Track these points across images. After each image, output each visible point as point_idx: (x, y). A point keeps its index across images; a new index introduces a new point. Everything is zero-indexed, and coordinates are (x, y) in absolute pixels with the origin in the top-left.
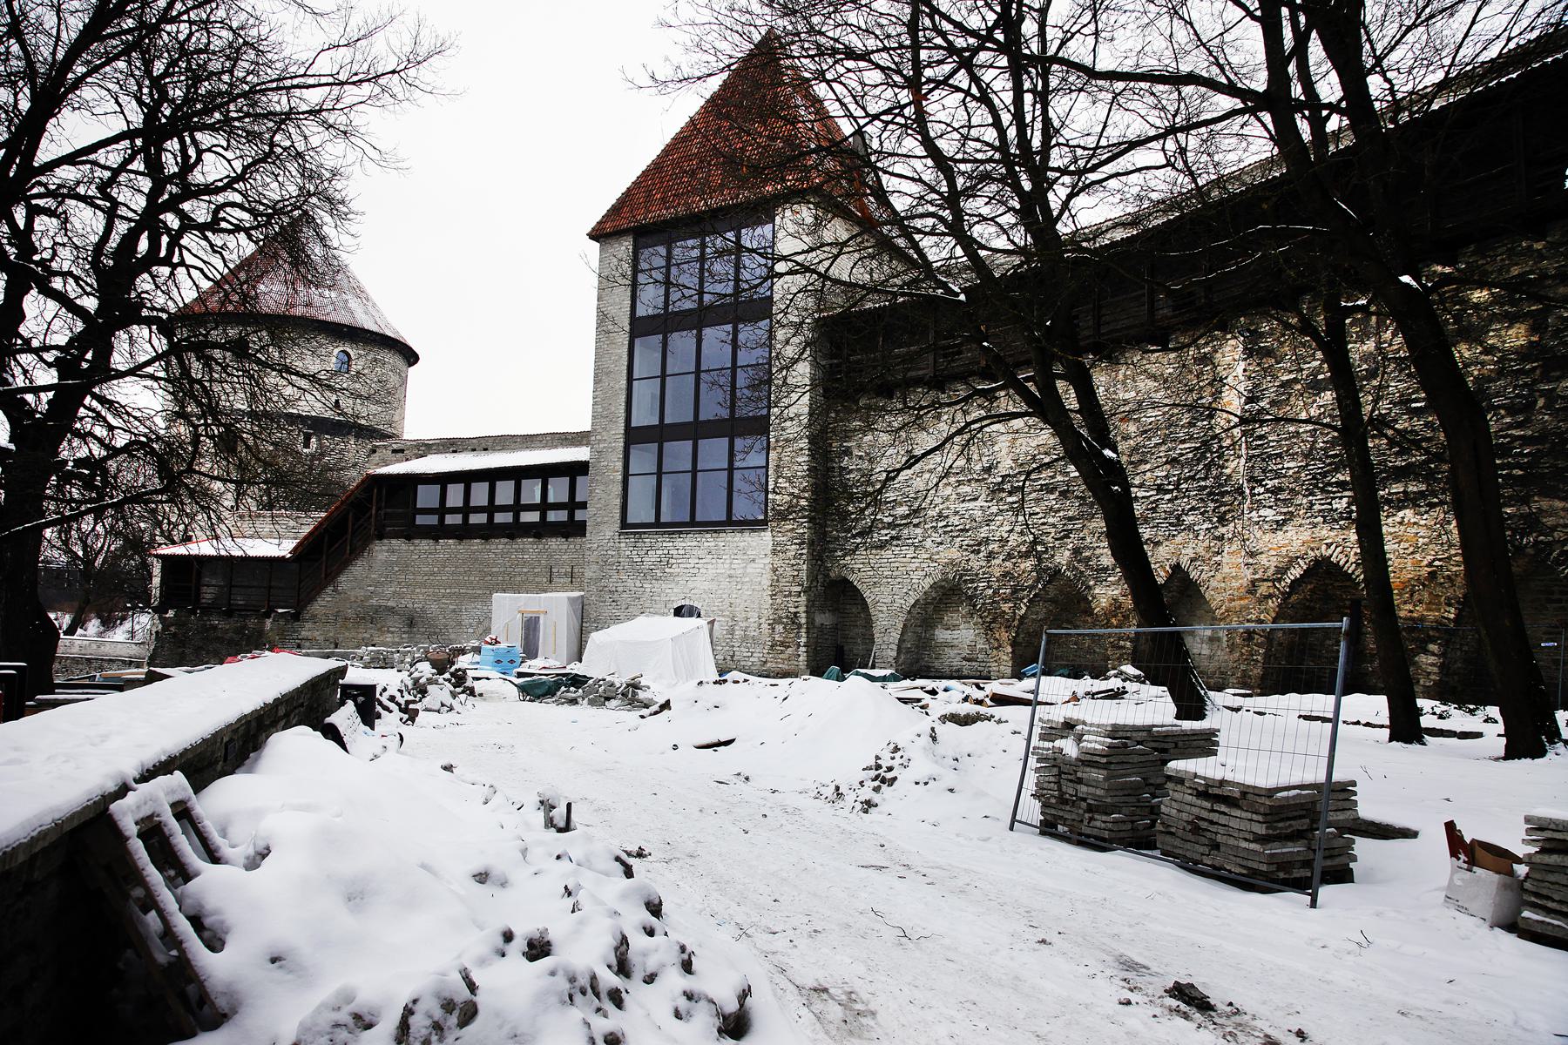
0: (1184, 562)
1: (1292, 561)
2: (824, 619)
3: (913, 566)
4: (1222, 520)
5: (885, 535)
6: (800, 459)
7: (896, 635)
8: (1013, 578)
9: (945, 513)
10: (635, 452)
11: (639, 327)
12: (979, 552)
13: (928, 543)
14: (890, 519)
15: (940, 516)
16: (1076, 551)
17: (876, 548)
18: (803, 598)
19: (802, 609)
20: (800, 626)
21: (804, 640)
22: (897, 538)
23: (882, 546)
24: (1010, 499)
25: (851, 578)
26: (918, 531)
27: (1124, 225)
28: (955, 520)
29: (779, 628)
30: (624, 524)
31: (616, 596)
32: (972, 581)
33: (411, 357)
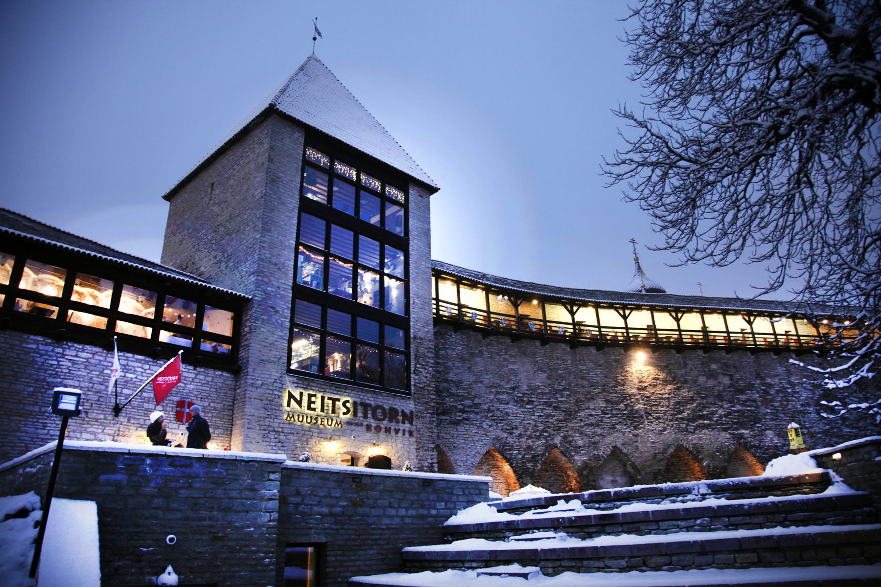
0: (619, 445)
1: (669, 446)
4: (636, 428)
5: (459, 416)
6: (430, 355)
8: (533, 450)
9: (492, 408)
12: (512, 433)
15: (489, 411)
16: (565, 437)
19: (435, 461)
22: (467, 419)
23: (457, 423)
24: (528, 406)
27: (492, 286)
31: (282, 437)
32: (510, 450)
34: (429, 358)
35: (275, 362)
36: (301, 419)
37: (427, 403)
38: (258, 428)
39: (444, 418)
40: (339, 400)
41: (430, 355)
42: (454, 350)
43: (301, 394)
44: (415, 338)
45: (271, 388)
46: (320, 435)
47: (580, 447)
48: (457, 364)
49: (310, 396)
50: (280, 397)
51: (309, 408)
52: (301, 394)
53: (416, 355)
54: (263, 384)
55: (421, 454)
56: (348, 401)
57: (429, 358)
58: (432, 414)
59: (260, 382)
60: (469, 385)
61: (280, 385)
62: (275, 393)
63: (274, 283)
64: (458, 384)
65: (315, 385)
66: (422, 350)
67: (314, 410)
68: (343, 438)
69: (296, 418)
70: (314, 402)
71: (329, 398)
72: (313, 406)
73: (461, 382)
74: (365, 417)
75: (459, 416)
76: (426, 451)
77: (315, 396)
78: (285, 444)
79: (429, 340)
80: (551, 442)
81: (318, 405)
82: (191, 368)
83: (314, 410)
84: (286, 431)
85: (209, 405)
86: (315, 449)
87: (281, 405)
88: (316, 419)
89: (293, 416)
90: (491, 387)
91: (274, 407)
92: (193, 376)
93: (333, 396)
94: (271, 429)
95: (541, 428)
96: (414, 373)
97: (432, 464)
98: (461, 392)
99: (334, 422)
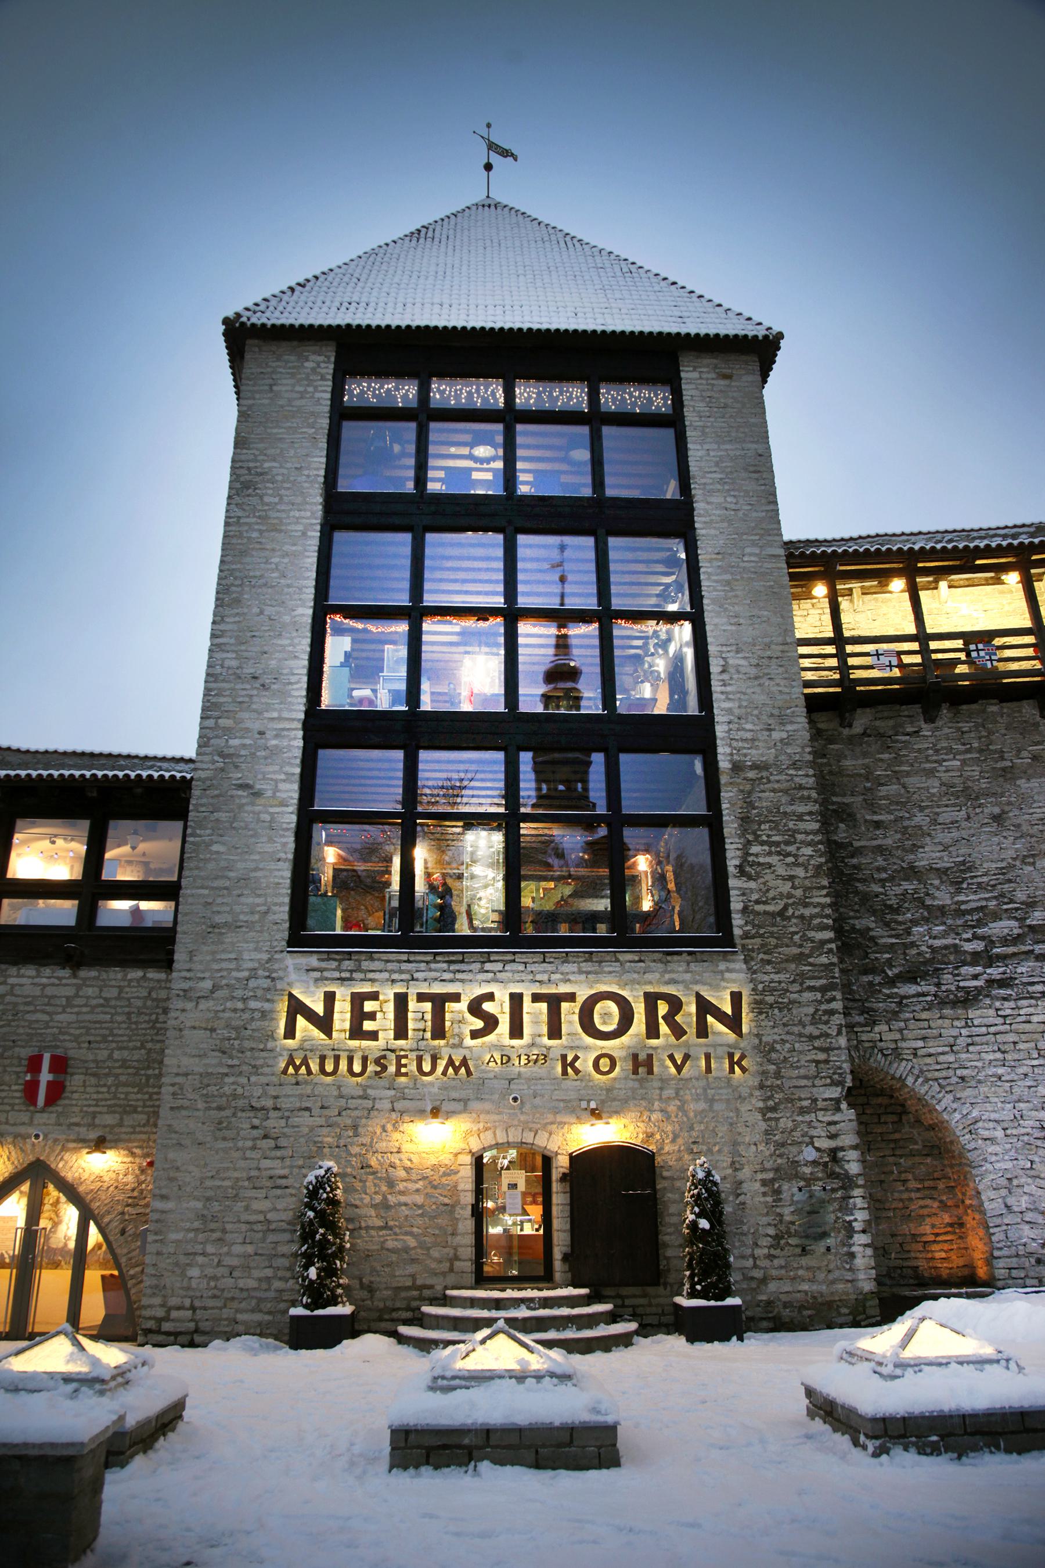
5: (972, 978)
6: (801, 809)
14: (978, 946)
17: (955, 1004)
18: (848, 1114)
19: (849, 1139)
20: (847, 1182)
21: (860, 1217)
22: (1004, 983)
23: (968, 999)
29: (790, 1190)
31: (274, 1123)
34: (800, 818)
35: (250, 925)
36: (329, 1068)
37: (800, 958)
38: (201, 1105)
39: (912, 989)
40: (456, 998)
41: (801, 809)
42: (931, 773)
43: (330, 999)
44: (737, 768)
45: (239, 993)
46: (398, 1105)
49: (358, 1000)
50: (266, 1015)
51: (356, 1032)
52: (330, 999)
53: (745, 820)
54: (215, 988)
55: (785, 1123)
56: (490, 997)
57: (800, 818)
58: (823, 989)
59: (208, 984)
60: (1002, 871)
61: (266, 983)
62: (253, 1004)
63: (248, 724)
64: (957, 876)
65: (377, 965)
66: (765, 799)
67: (373, 1035)
68: (474, 1105)
69: (314, 1067)
70: (372, 1016)
71: (421, 998)
72: (368, 1026)
73: (966, 867)
75: (972, 978)
76: (803, 1111)
77: (374, 996)
78: (282, 1142)
79: (794, 765)
81: (384, 1022)
82: (66, 973)
83: (373, 1035)
84: (285, 1104)
85: (110, 1057)
86: (382, 1146)
87: (272, 1036)
88: (377, 1062)
89: (305, 1062)
91: (247, 1044)
92: (70, 992)
93: (438, 989)
94: (241, 1103)
96: (742, 872)
97: (833, 1152)
98: (972, 899)
99: (441, 1065)
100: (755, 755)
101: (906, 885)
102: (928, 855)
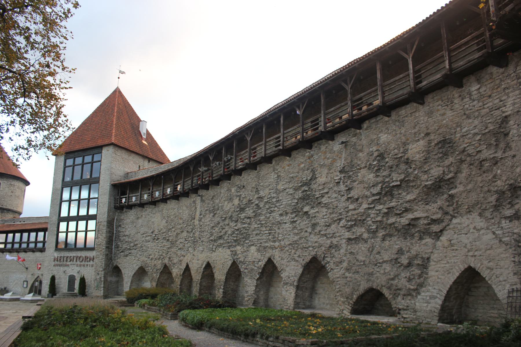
2: (114, 279)
3: (134, 262)
7: (129, 284)
10: (61, 224)
11: (65, 184)
13: (138, 255)
14: (129, 247)
15: (142, 247)
16: (170, 258)
18: (103, 272)
19: (103, 276)
21: (102, 286)
23: (127, 256)
25: (119, 266)
26: (136, 251)
28: (144, 248)
30: (57, 248)
33: (27, 183)
47: (175, 264)
48: (130, 226)
73: (130, 235)
74: (76, 261)
80: (164, 262)
90: (144, 234)
95: (160, 254)
98: (130, 240)
100: (101, 220)
101: (124, 238)
102: (127, 233)
